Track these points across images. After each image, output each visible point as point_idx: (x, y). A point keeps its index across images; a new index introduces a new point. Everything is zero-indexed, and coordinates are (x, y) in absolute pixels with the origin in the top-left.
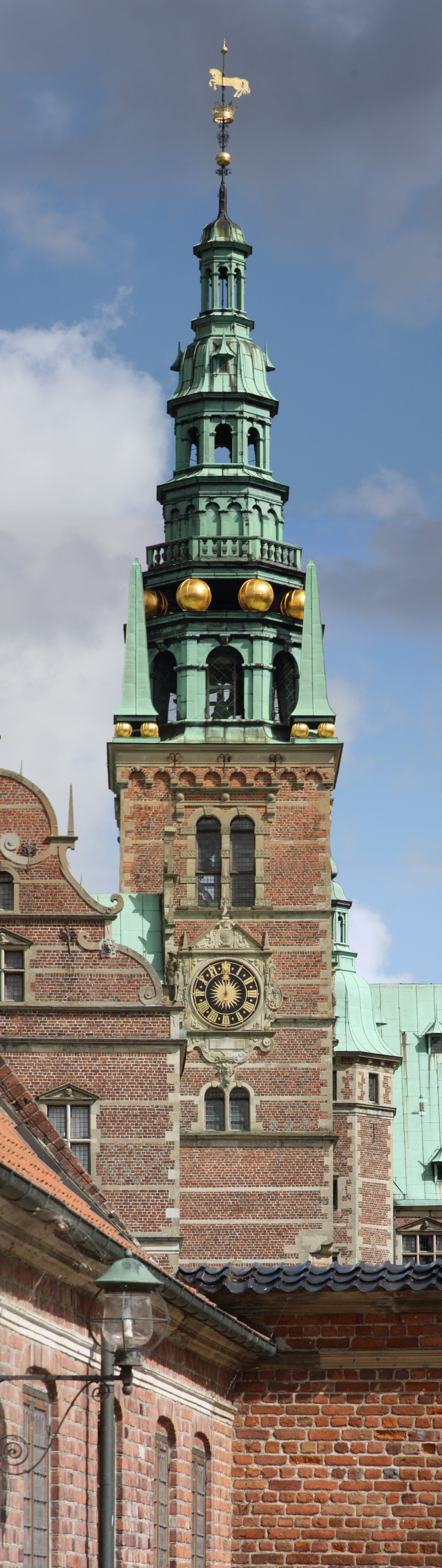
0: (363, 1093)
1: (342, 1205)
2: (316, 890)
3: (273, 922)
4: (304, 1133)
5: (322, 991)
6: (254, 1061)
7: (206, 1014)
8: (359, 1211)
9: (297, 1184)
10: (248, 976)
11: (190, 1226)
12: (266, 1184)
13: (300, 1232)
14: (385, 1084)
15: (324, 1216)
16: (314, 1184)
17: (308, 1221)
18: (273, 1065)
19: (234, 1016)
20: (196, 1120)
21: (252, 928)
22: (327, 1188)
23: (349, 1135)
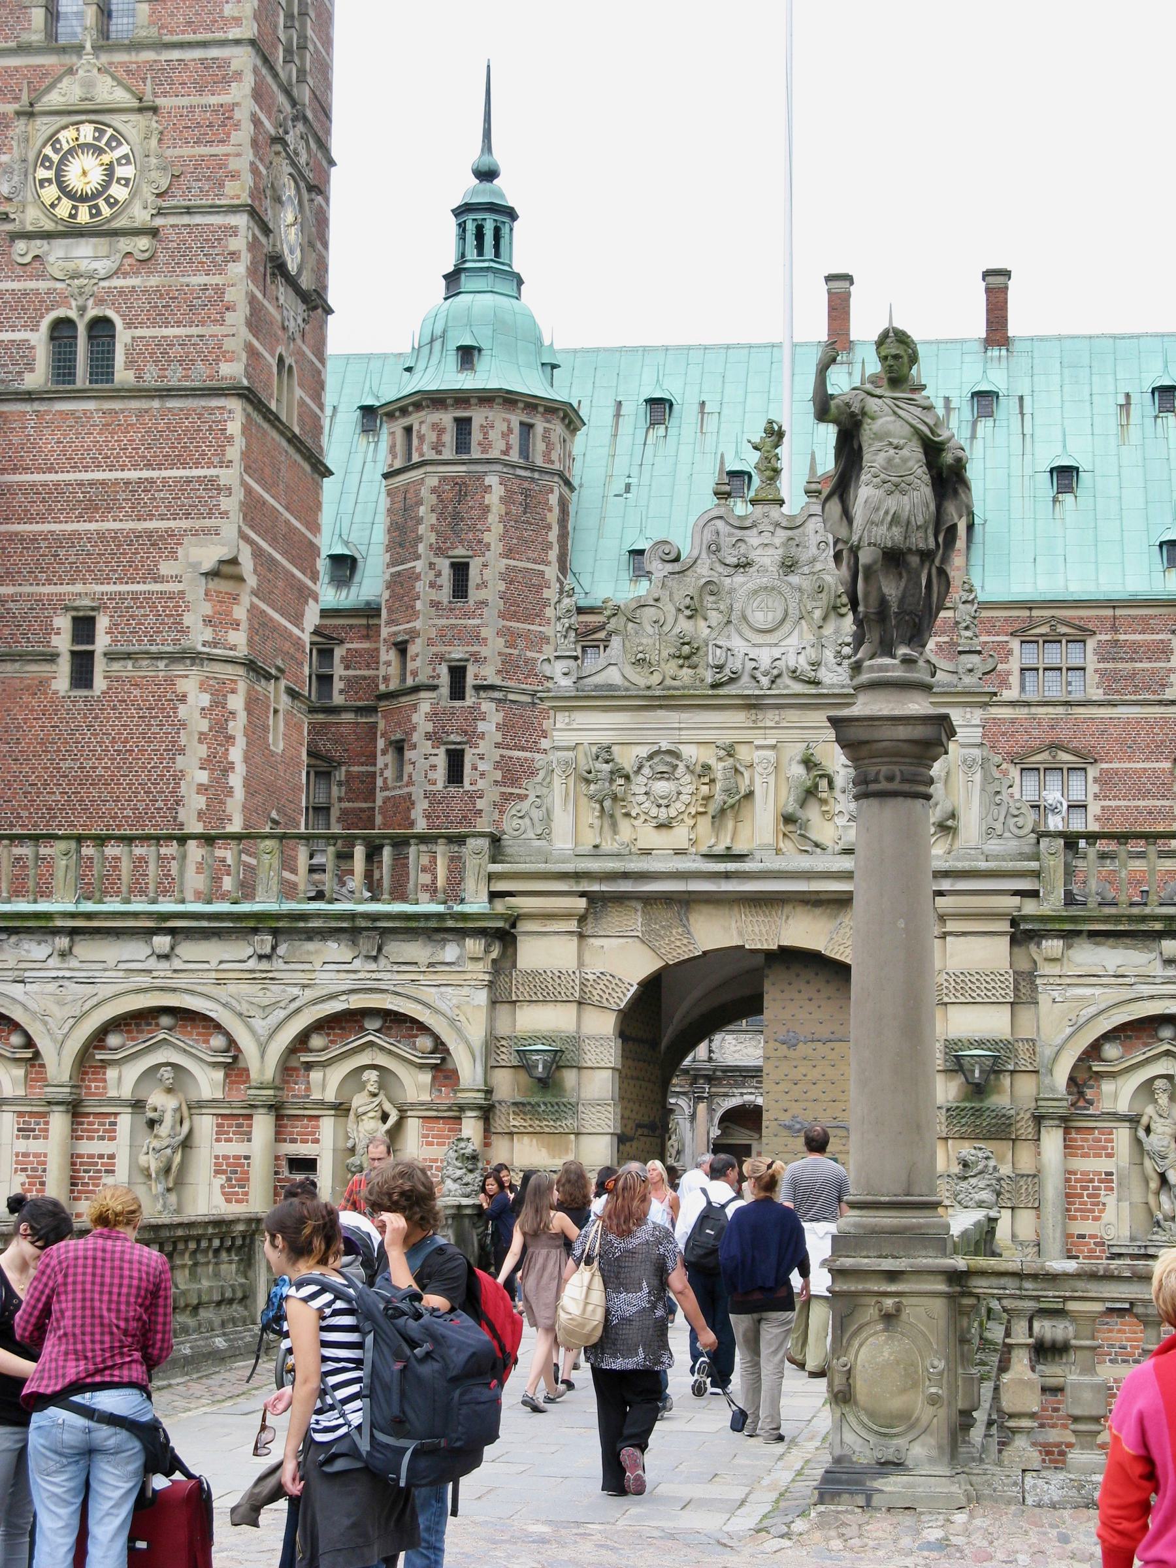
0: (509, 447)
1: (474, 595)
2: (229, 10)
3: (160, 61)
4: (197, 384)
5: (233, 164)
6: (125, 275)
7: (53, 206)
8: (498, 604)
9: (185, 465)
10: (120, 144)
11: (17, 534)
12: (135, 466)
13: (186, 540)
14: (546, 438)
15: (225, 514)
16: (210, 465)
17: (198, 524)
18: (154, 281)
19: (96, 206)
20: (32, 370)
21: (128, 72)
22: (230, 471)
23: (486, 502)
